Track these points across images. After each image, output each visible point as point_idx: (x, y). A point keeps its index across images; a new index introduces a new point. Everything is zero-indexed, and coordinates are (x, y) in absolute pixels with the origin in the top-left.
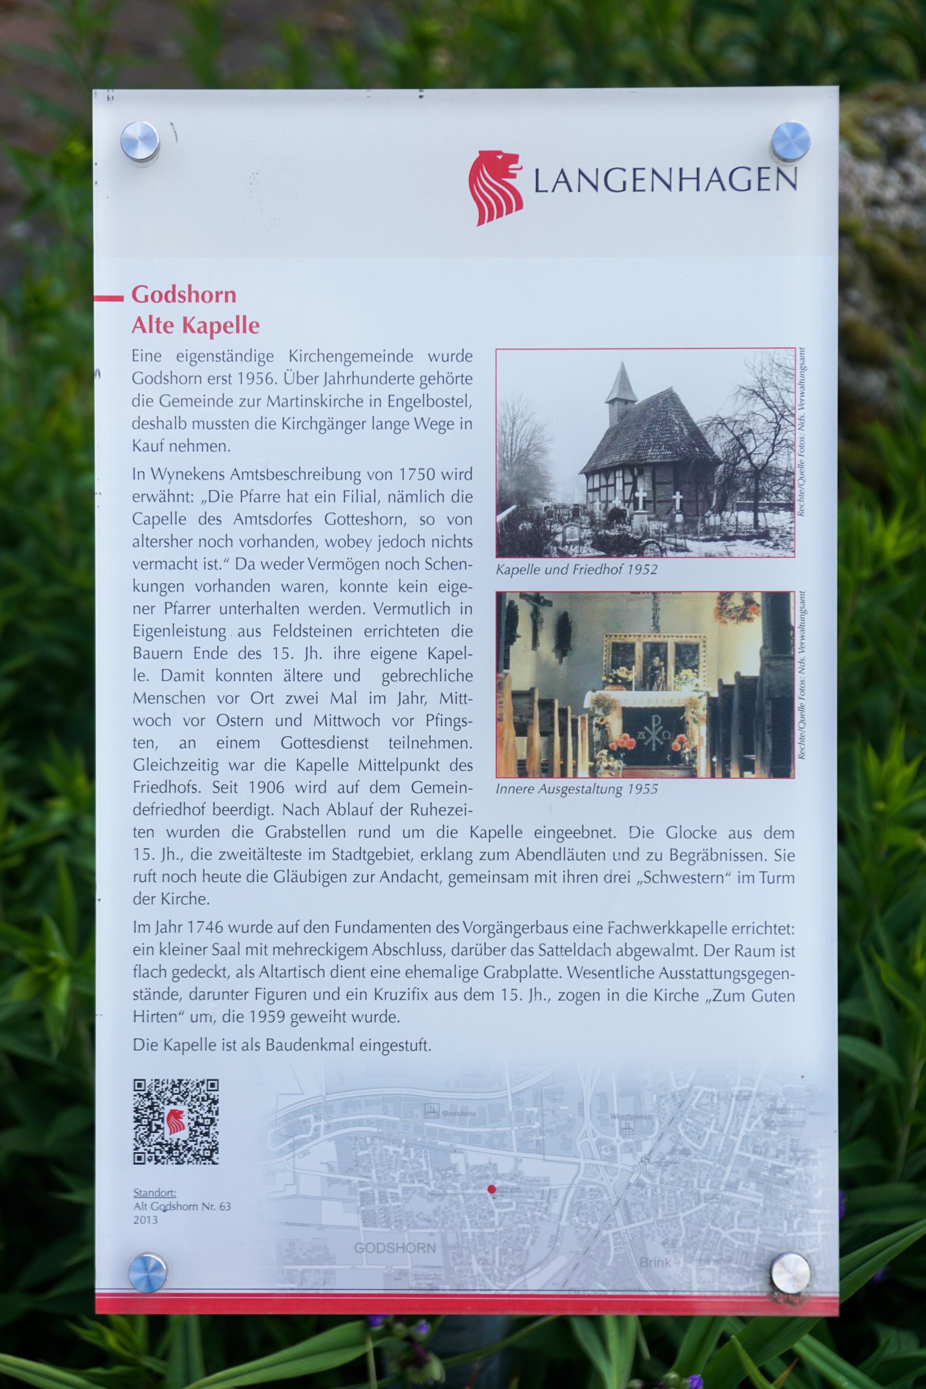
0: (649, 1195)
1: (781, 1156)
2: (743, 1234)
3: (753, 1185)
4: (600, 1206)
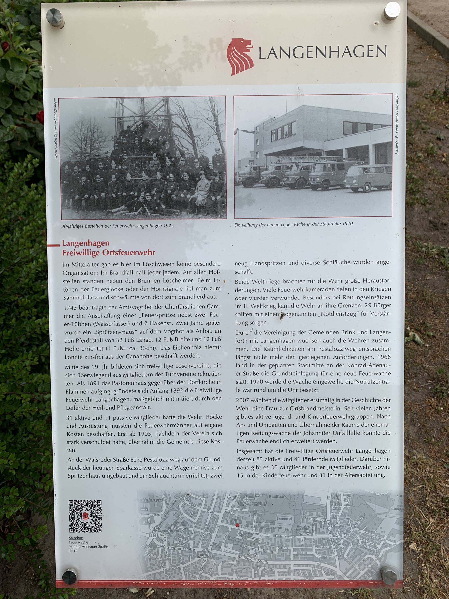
0: (160, 553)
1: (250, 526)
3: (231, 546)
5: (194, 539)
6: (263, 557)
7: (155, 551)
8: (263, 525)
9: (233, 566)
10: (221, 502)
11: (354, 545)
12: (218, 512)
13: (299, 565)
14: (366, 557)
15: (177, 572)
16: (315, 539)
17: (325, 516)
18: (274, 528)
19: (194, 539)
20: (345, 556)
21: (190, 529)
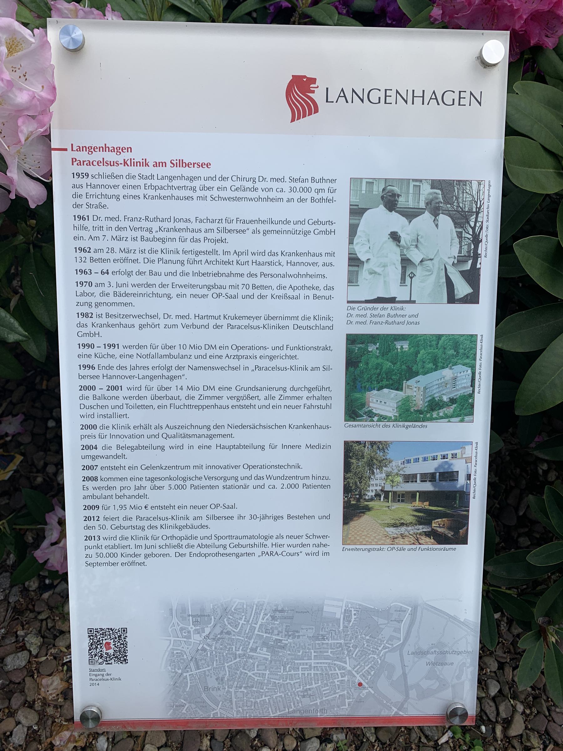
0: (209, 655)
1: (280, 634)
2: (260, 674)
3: (265, 649)
4: (182, 661)
5: (236, 644)
6: (290, 657)
7: (205, 654)
8: (290, 633)
10: (257, 617)
11: (361, 648)
12: (255, 624)
13: (318, 663)
14: (370, 657)
16: (331, 644)
17: (339, 627)
18: (299, 636)
19: (236, 644)
20: (354, 656)
21: (233, 637)
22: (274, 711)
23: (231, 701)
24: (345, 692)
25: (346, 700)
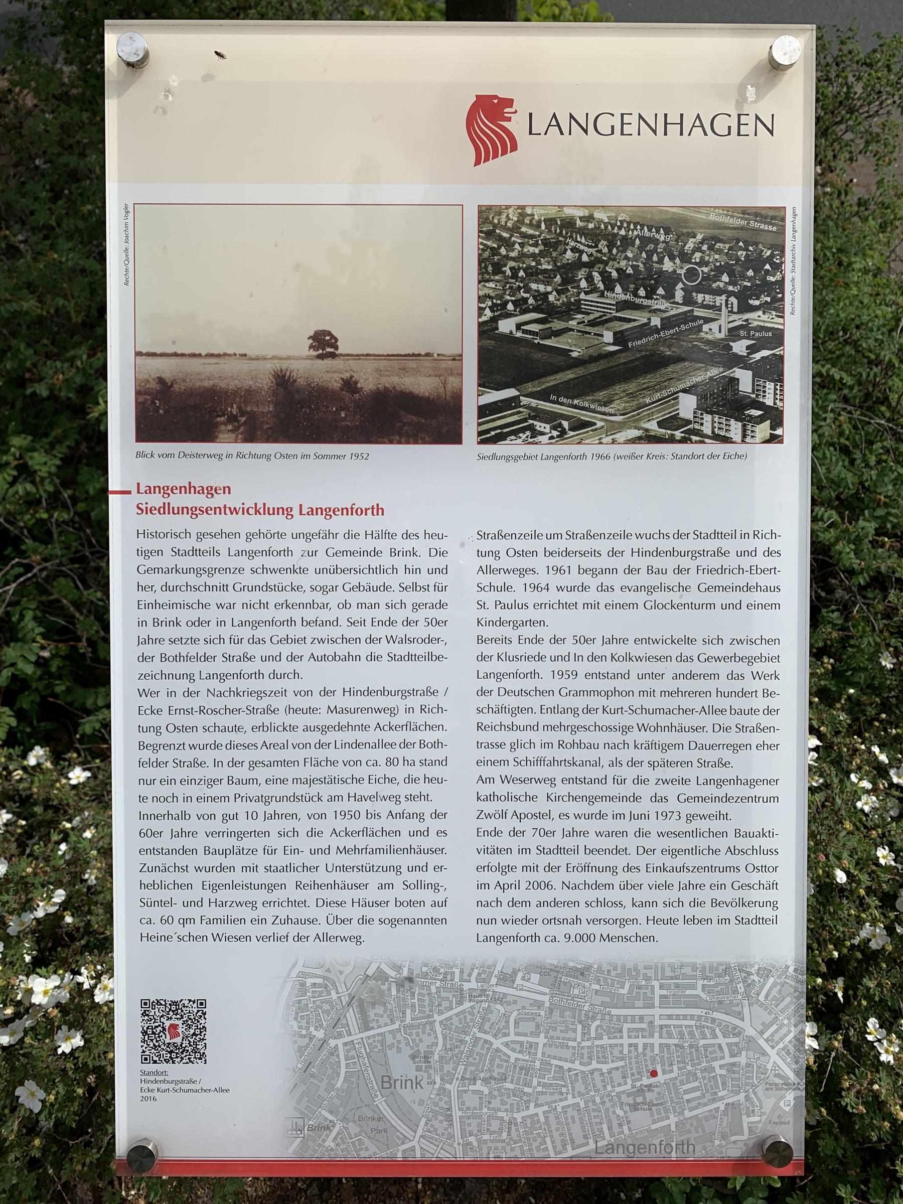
2: (522, 1043)
3: (535, 977)
4: (326, 1007)
6: (598, 1000)
9: (538, 1019)
13: (670, 1017)
15: (428, 1030)
20: (762, 998)
22: (559, 1148)
23: (449, 1118)
24: (741, 1097)
25: (744, 1117)
